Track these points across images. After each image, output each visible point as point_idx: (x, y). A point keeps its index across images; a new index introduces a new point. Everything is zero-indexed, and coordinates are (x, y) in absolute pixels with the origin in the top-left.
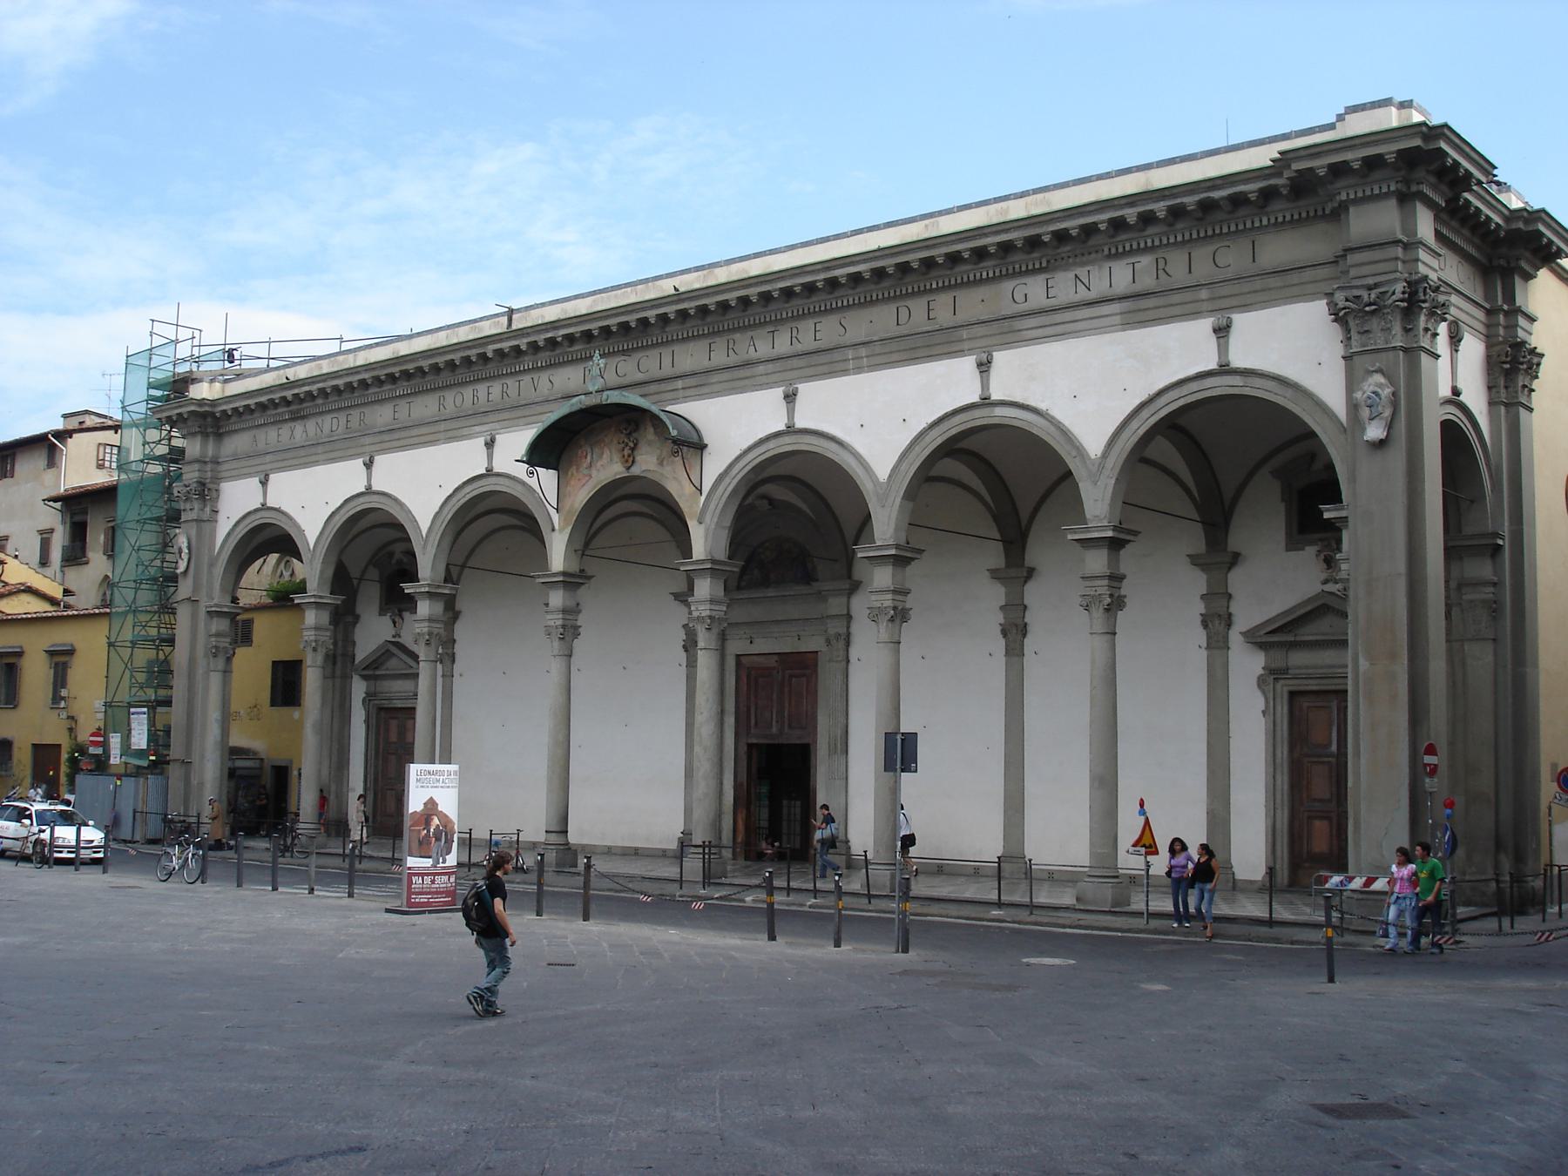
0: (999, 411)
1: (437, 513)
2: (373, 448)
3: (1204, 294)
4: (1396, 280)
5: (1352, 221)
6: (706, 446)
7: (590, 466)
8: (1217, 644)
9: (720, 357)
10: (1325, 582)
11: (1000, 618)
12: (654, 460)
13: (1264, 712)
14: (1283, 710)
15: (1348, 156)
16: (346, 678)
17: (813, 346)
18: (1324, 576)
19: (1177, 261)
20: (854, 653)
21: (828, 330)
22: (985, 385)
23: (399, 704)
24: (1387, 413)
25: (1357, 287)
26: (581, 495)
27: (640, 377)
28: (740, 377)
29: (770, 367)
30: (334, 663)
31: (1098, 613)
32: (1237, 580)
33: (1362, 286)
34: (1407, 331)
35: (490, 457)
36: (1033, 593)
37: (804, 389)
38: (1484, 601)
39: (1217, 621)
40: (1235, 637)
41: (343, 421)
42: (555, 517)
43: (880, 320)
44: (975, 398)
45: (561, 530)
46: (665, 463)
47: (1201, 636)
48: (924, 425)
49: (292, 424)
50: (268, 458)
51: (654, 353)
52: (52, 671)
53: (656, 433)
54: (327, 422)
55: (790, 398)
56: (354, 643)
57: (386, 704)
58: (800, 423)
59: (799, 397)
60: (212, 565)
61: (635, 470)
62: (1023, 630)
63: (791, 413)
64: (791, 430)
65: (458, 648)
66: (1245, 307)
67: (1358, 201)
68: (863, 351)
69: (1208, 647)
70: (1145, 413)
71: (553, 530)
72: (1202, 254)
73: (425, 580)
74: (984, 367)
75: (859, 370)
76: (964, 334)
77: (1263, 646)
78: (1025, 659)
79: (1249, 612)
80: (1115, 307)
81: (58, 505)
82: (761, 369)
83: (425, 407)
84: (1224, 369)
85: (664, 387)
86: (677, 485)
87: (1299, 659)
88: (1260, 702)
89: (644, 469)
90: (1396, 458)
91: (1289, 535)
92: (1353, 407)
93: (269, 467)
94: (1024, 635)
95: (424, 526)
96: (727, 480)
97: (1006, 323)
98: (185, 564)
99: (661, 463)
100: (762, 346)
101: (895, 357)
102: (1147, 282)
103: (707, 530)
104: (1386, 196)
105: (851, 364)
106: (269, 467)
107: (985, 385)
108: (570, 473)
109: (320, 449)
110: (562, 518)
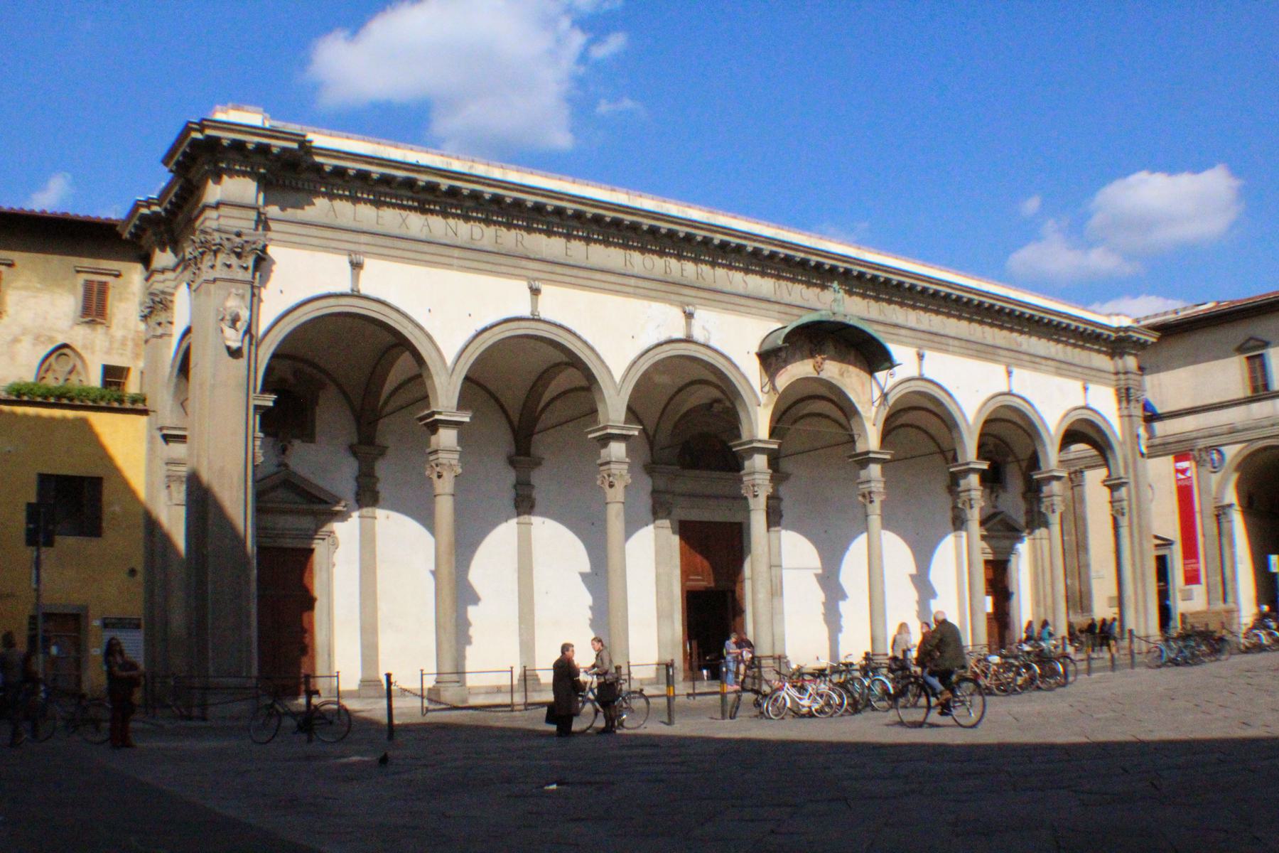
2: (536, 275)
46: (845, 375)
50: (364, 238)
61: (824, 375)
73: (613, 421)
75: (954, 353)
76: (1002, 352)
82: (903, 332)
83: (639, 261)
89: (829, 374)
93: (363, 248)
95: (618, 376)
97: (1017, 355)
99: (842, 375)
101: (970, 352)
103: (878, 430)
106: (363, 248)
109: (456, 253)
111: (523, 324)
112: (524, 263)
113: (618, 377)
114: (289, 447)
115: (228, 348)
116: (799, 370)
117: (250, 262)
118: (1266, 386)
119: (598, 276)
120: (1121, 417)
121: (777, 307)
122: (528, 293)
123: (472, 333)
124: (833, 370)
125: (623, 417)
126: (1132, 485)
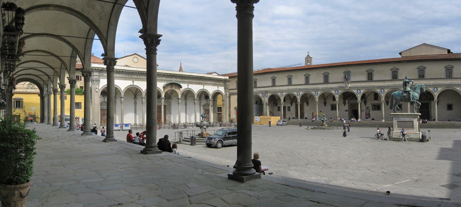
7: (167, 87)
8: (200, 106)
9: (181, 80)
26: (166, 90)
28: (184, 82)
32: (201, 102)
36: (187, 101)
37: (189, 85)
39: (200, 104)
40: (201, 106)
44: (203, 88)
55: (188, 85)
57: (103, 109)
58: (189, 88)
65: (117, 102)
75: (194, 84)
79: (202, 104)
84: (218, 90)
86: (177, 90)
87: (205, 107)
88: (203, 110)
112: (132, 79)
113: (144, 91)
115: (96, 91)
116: (169, 88)
117: (98, 82)
118: (256, 86)
119: (141, 79)
120: (225, 91)
123: (125, 87)
124: (174, 88)
125: (144, 95)
126: (225, 101)
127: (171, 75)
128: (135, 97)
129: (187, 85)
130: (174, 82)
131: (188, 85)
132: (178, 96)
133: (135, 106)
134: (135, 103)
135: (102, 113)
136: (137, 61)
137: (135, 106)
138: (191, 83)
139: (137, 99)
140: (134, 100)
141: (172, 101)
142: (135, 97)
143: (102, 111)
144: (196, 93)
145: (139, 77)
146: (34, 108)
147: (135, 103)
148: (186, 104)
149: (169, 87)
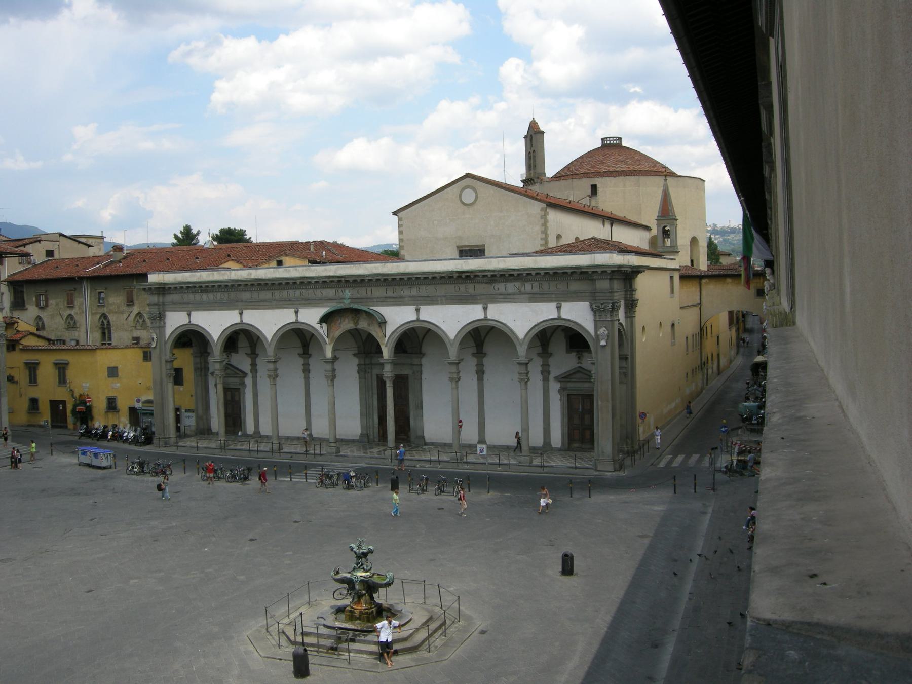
0: (490, 322)
1: (275, 334)
3: (553, 296)
4: (609, 303)
5: (597, 283)
6: (386, 322)
7: (340, 324)
8: (546, 379)
9: (390, 293)
10: (578, 363)
11: (475, 368)
12: (366, 324)
13: (560, 400)
14: (566, 399)
15: (598, 270)
16: (206, 376)
17: (426, 295)
18: (577, 362)
19: (545, 285)
20: (423, 377)
21: (431, 290)
22: (486, 314)
23: (232, 386)
24: (606, 338)
25: (597, 303)
26: (337, 333)
27: (359, 296)
28: (399, 301)
29: (410, 299)
30: (201, 370)
31: (523, 383)
32: (551, 361)
33: (600, 303)
34: (611, 315)
35: (297, 316)
36: (486, 361)
37: (423, 308)
38: (624, 373)
39: (545, 373)
40: (551, 377)
41: (226, 296)
42: (327, 340)
43: (450, 289)
44: (482, 317)
45: (330, 344)
47: (541, 377)
48: (465, 324)
49: (201, 294)
51: (364, 289)
52: (57, 371)
53: (366, 315)
54: (219, 295)
55: (418, 310)
56: (208, 363)
58: (421, 318)
59: (420, 310)
60: (166, 343)
61: (359, 327)
62: (483, 372)
63: (418, 315)
64: (418, 320)
65: (258, 367)
66: (565, 301)
67: (598, 279)
68: (444, 299)
69: (543, 380)
70: (536, 328)
71: (326, 343)
72: (553, 284)
74: (485, 309)
75: (442, 304)
77: (560, 381)
78: (484, 381)
79: (555, 372)
80: (527, 296)
81: (6, 283)
82: (407, 299)
85: (369, 300)
86: (375, 332)
87: (570, 385)
88: (559, 397)
89: (362, 326)
90: (608, 350)
91: (567, 349)
92: (597, 336)
94: (484, 374)
96: (395, 333)
98: (155, 343)
100: (406, 292)
102: (536, 290)
103: (388, 349)
104: (607, 279)
105: (439, 302)
107: (486, 314)
108: (332, 325)
109: (216, 305)
110: (330, 340)
111: (238, 325)
113: (269, 339)
114: (229, 356)
116: (346, 324)
121: (336, 301)
122: (239, 314)
127: (343, 279)
128: (306, 353)
129: (413, 308)
130: (347, 307)
131: (418, 310)
132: (379, 352)
133: (307, 379)
134: (306, 370)
135: (229, 398)
136: (472, 200)
137: (307, 379)
138: (432, 300)
139: (310, 356)
140: (301, 361)
141: (424, 361)
142: (306, 353)
143: (229, 393)
144: (452, 335)
145: (255, 295)
146: (88, 385)
147: (306, 370)
148: (480, 373)
149: (347, 321)
